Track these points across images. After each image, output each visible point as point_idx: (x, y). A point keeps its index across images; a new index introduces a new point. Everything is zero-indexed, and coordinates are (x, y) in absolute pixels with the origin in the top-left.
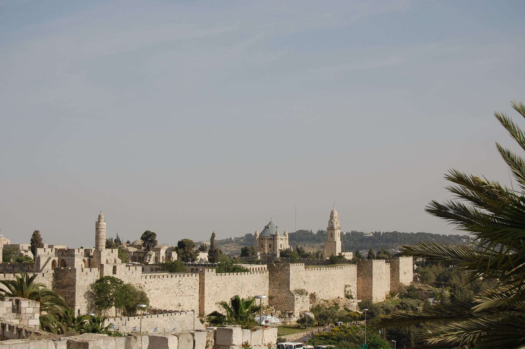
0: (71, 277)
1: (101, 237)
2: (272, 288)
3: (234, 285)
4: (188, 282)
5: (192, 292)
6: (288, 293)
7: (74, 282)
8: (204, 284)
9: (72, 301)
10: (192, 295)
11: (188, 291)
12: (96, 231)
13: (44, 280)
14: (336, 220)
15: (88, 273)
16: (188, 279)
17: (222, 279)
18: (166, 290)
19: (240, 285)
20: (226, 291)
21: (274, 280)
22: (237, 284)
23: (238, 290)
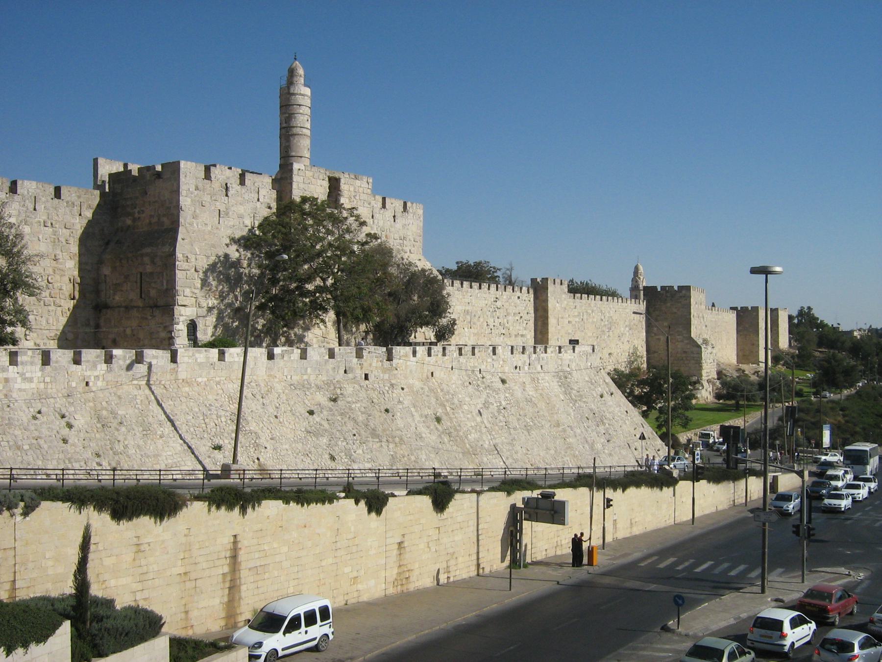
1: (295, 131)
2: (655, 334)
4: (513, 304)
5: (522, 328)
8: (546, 310)
9: (165, 286)
10: (522, 336)
11: (515, 324)
12: (282, 113)
13: (61, 211)
14: (642, 278)
16: (513, 297)
17: (575, 306)
18: (468, 317)
19: (606, 323)
22: (602, 320)
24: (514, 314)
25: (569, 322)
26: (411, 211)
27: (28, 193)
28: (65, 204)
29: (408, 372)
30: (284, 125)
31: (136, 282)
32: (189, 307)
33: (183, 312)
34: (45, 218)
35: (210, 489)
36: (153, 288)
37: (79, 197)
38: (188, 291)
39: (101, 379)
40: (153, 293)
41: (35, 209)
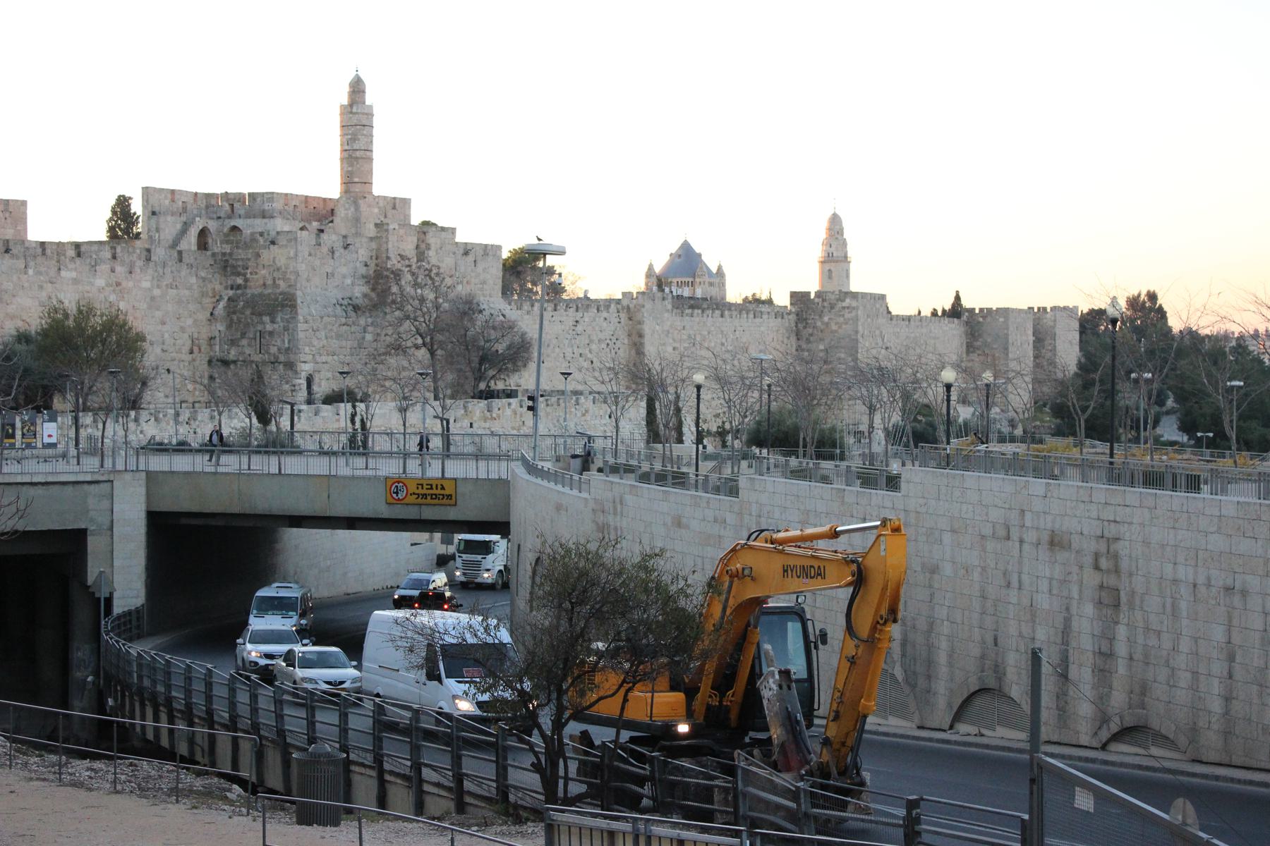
4: (597, 328)
7: (289, 279)
8: (641, 336)
9: (287, 345)
13: (183, 273)
17: (684, 327)
19: (730, 348)
21: (811, 338)
25: (674, 349)
26: (490, 253)
30: (346, 148)
31: (255, 339)
36: (274, 345)
37: (196, 259)
38: (307, 349)
40: (274, 350)
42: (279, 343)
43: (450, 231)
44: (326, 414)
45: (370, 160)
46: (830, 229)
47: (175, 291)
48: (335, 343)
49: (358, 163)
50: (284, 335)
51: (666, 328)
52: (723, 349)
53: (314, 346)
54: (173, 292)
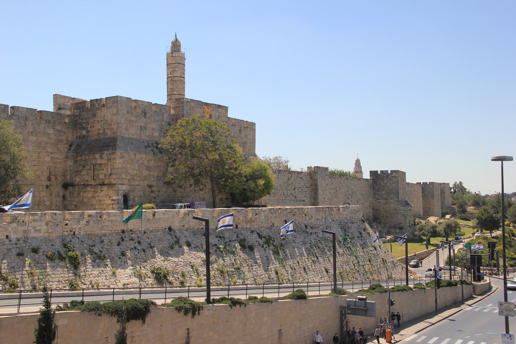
0: (106, 119)
1: (176, 78)
2: (378, 199)
3: (345, 192)
6: (396, 203)
7: (113, 128)
8: (316, 185)
9: (110, 172)
10: (303, 201)
11: (299, 194)
12: (168, 68)
13: (42, 126)
15: (147, 113)
17: (333, 183)
19: (350, 193)
20: (337, 198)
21: (379, 190)
22: (347, 191)
23: (348, 198)
24: (299, 188)
25: (330, 192)
26: (249, 127)
27: (21, 115)
28: (45, 121)
29: (260, 222)
30: (170, 76)
31: (90, 170)
32: (125, 185)
33: (120, 188)
34: (32, 130)
35: (171, 300)
36: (102, 173)
37: (53, 118)
39: (82, 230)
40: (102, 176)
41: (26, 125)
42: (105, 172)
43: (224, 108)
44: (114, 218)
45: (184, 83)
46: (356, 164)
47: (35, 137)
48: (145, 173)
49: (176, 84)
50: (108, 165)
51: (327, 183)
52: (348, 193)
53: (130, 173)
54: (33, 138)
